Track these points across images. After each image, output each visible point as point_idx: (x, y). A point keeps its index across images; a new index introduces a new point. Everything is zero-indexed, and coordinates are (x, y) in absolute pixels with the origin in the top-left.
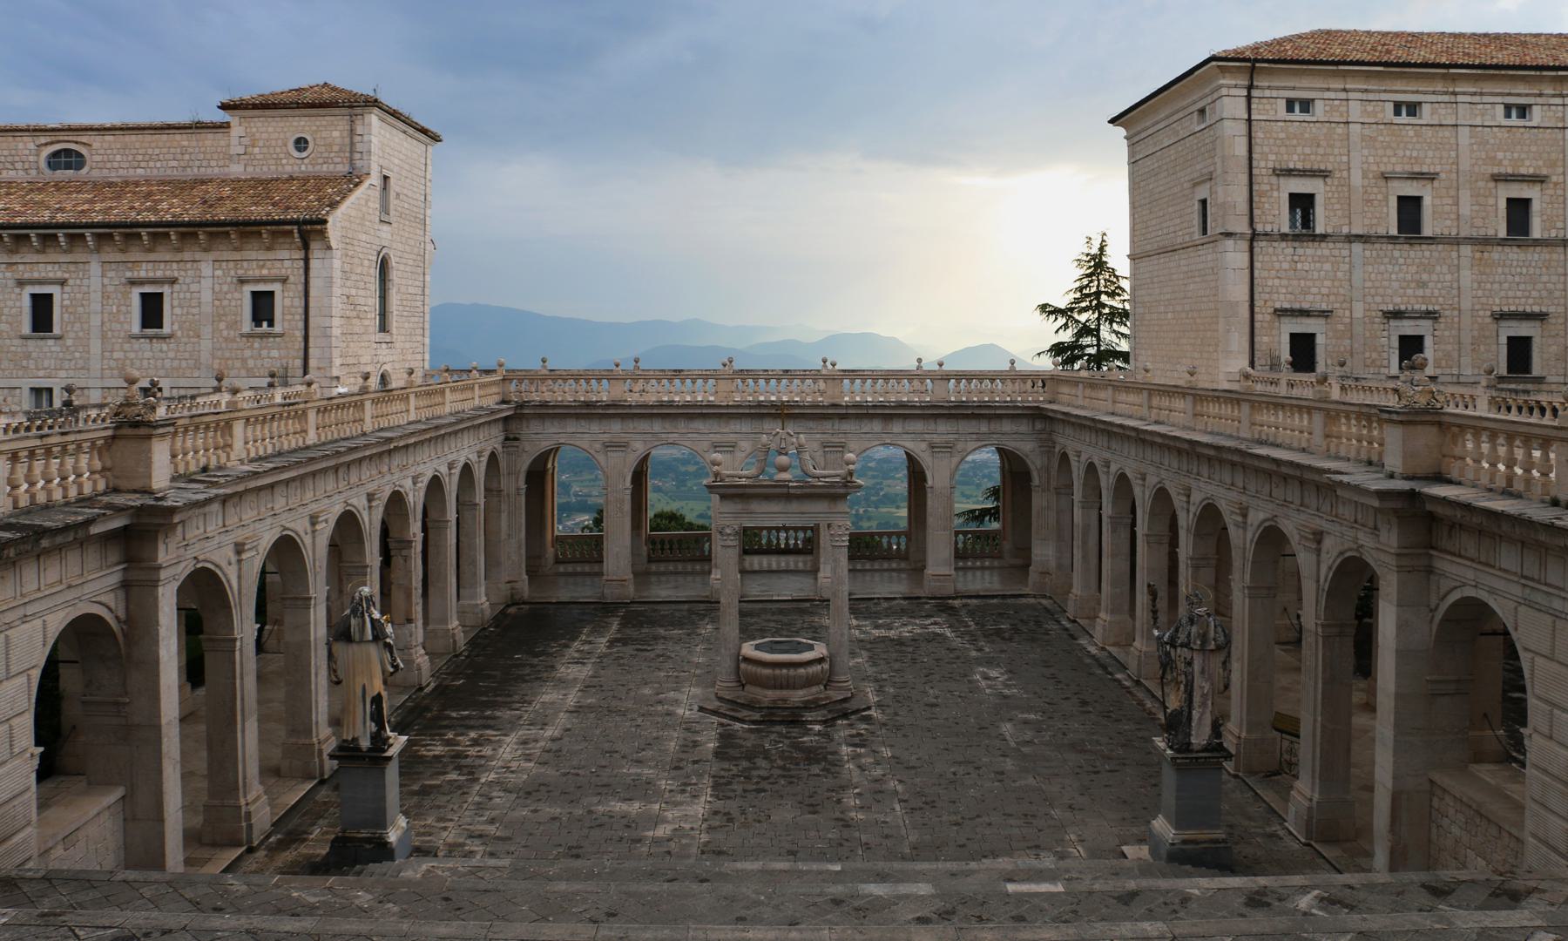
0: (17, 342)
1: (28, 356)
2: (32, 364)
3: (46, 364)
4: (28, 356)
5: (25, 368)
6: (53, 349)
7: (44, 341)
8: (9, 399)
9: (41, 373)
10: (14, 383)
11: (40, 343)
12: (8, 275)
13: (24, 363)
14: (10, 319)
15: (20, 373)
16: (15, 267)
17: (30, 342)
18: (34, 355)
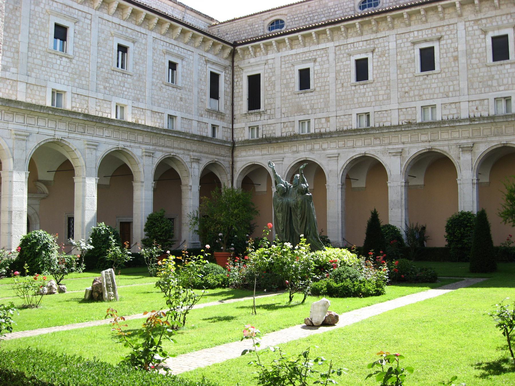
0: (484, 69)
1: (492, 78)
2: (495, 83)
3: (505, 81)
4: (492, 78)
5: (490, 86)
6: (509, 71)
7: (503, 66)
8: (480, 108)
9: (502, 88)
10: (483, 96)
11: (500, 68)
12: (476, 27)
13: (490, 83)
14: (478, 55)
15: (487, 89)
16: (479, 22)
17: (493, 69)
18: (496, 77)
